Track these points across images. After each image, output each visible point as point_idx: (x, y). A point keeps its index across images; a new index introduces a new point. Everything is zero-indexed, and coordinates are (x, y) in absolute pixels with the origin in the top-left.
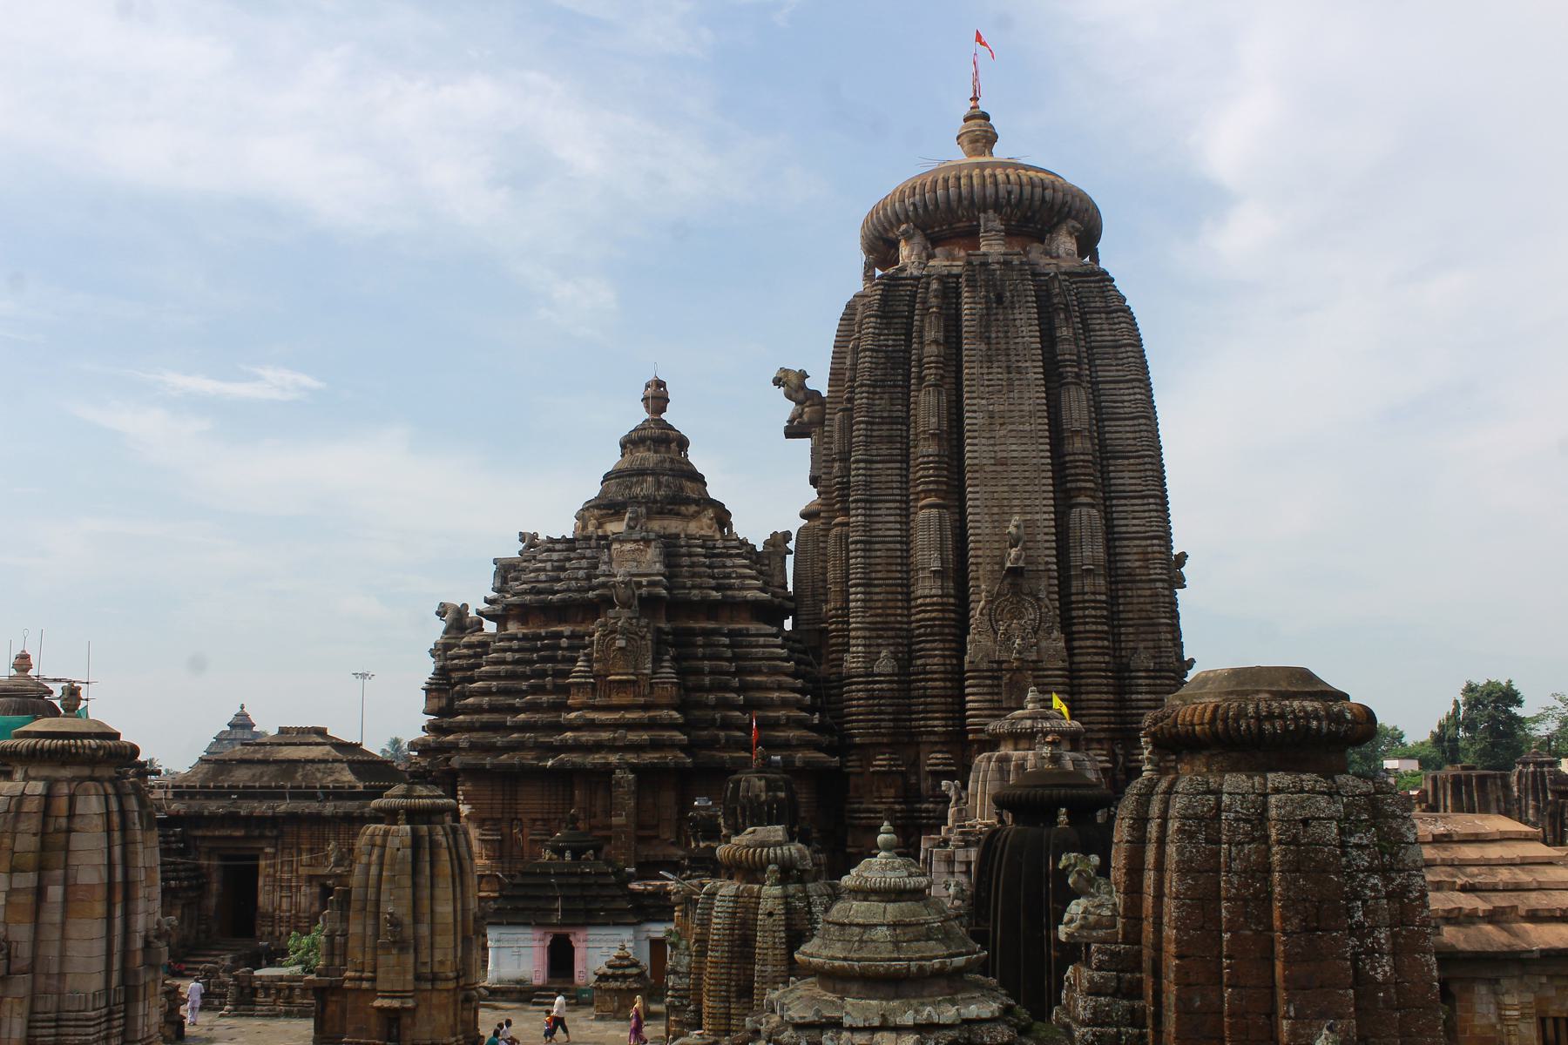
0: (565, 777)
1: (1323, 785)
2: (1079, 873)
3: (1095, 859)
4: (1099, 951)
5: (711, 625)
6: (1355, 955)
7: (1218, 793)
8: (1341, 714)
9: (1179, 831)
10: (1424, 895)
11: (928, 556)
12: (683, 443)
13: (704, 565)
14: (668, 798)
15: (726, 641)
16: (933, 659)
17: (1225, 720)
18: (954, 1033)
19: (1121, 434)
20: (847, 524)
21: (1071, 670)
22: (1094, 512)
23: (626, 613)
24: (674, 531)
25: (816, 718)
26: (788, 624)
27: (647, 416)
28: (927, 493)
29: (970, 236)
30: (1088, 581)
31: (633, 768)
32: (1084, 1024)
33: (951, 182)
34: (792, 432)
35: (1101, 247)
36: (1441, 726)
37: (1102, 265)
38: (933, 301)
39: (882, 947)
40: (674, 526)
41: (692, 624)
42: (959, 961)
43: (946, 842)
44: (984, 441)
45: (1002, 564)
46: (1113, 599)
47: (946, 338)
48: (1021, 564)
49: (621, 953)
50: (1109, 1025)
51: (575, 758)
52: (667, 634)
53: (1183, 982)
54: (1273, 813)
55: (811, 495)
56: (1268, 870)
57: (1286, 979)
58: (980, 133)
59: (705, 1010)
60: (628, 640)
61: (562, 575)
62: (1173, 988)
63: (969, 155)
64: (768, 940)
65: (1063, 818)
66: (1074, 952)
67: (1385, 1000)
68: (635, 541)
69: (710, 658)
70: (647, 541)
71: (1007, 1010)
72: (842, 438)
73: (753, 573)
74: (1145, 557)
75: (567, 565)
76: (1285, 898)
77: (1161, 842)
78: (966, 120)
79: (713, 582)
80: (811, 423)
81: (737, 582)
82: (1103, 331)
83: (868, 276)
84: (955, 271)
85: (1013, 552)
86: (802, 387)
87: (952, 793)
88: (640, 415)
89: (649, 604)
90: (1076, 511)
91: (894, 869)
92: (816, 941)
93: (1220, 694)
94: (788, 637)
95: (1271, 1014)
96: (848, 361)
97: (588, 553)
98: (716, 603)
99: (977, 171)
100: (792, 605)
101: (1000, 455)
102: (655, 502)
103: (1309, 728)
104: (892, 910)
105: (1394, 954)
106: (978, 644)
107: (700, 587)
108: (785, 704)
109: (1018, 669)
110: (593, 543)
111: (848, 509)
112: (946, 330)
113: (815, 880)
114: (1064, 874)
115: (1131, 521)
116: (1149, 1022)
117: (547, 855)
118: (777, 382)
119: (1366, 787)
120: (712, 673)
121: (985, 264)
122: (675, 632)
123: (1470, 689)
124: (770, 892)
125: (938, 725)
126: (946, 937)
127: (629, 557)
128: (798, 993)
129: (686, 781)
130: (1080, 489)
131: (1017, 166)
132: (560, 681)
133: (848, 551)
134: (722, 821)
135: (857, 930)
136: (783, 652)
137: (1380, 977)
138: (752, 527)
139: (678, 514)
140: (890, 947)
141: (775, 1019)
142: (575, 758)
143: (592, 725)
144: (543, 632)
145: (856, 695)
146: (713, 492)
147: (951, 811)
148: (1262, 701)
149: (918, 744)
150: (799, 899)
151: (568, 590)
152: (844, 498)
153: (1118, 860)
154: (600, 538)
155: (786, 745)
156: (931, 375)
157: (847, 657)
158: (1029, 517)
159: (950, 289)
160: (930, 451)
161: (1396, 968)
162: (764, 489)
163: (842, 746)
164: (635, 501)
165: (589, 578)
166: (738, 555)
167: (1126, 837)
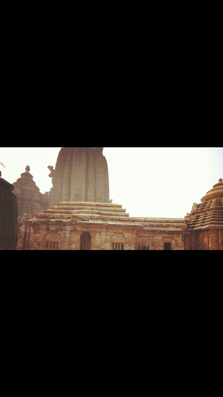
12: (32, 177)
34: (50, 176)
48: (78, 193)
70: (18, 188)
88: (25, 171)
101: (77, 176)
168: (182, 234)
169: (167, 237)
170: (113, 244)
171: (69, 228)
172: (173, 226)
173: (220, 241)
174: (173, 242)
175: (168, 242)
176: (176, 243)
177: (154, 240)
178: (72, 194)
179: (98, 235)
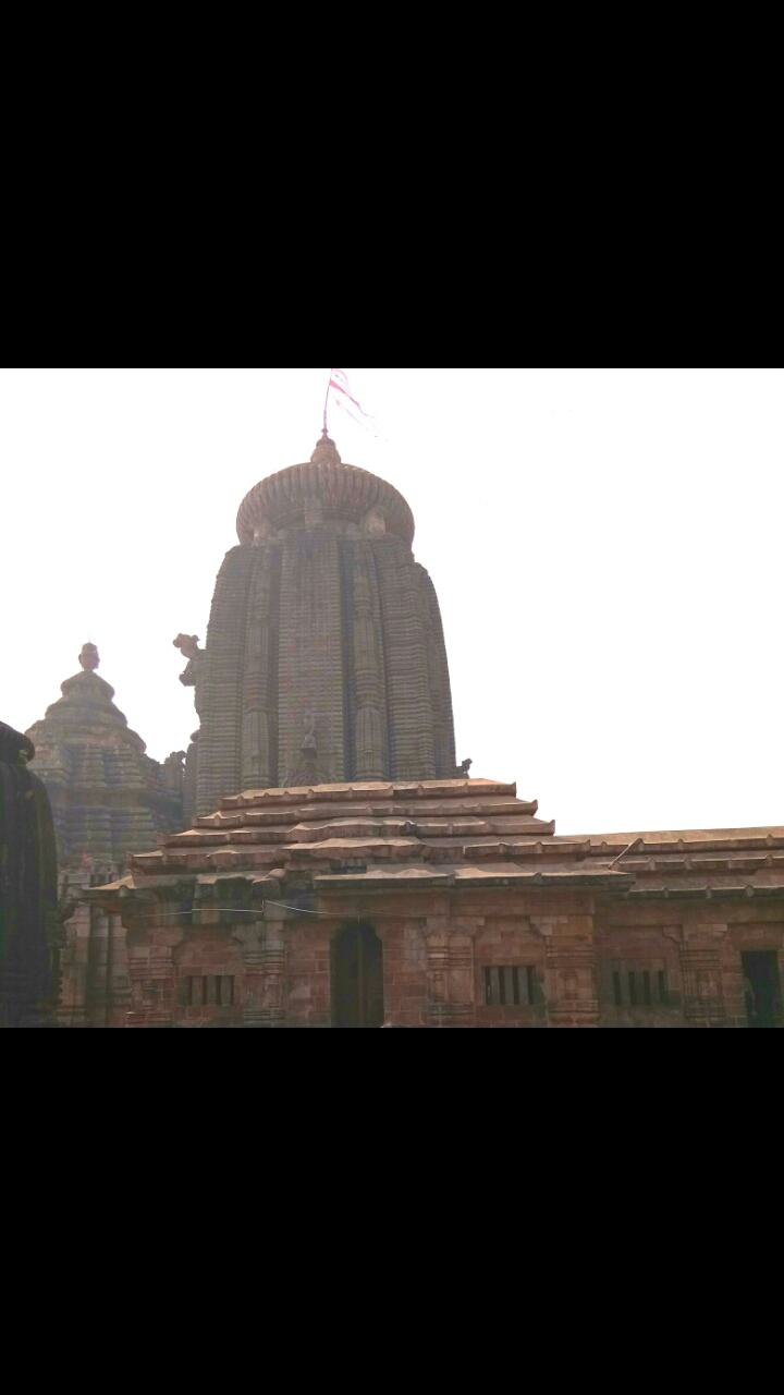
12: (107, 691)
22: (374, 711)
34: (186, 679)
44: (292, 659)
48: (311, 746)
70: (51, 746)
88: (78, 669)
130: (366, 695)
158: (323, 714)
170: (487, 970)
171: (277, 909)
177: (686, 939)
178: (284, 750)
179: (411, 934)
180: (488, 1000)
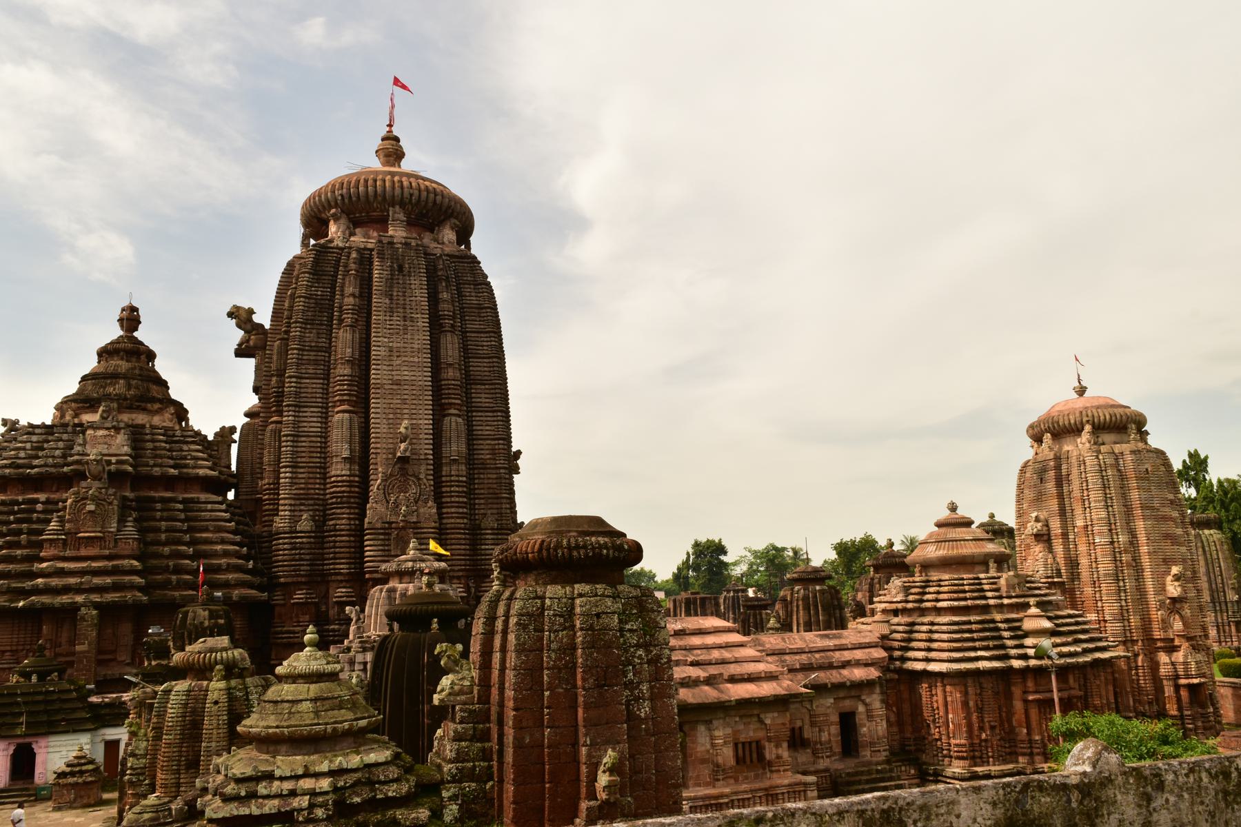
0: (34, 615)
1: (609, 591)
2: (449, 657)
3: (460, 647)
4: (461, 710)
5: (168, 495)
6: (628, 704)
7: (543, 598)
8: (621, 545)
9: (517, 624)
10: (669, 660)
11: (340, 447)
12: (151, 356)
13: (165, 449)
14: (126, 629)
15: (181, 506)
16: (342, 520)
17: (548, 549)
18: (358, 775)
19: (480, 367)
20: (281, 422)
21: (440, 529)
22: (460, 420)
23: (97, 484)
24: (140, 422)
25: (251, 564)
26: (231, 495)
27: (121, 333)
28: (342, 402)
29: (382, 223)
30: (454, 467)
31: (96, 606)
32: (450, 761)
33: (370, 182)
34: (240, 353)
35: (473, 239)
36: (679, 569)
37: (473, 252)
38: (353, 266)
39: (306, 716)
40: (141, 418)
41: (153, 494)
42: (363, 723)
43: (349, 649)
45: (394, 454)
46: (471, 479)
47: (361, 293)
48: (408, 454)
49: (80, 754)
50: (468, 761)
51: (46, 599)
52: (132, 501)
53: (518, 727)
54: (578, 610)
55: (254, 400)
56: (574, 648)
57: (585, 720)
58: (392, 151)
59: (159, 782)
60: (97, 505)
61: (40, 454)
62: (511, 731)
63: (384, 165)
64: (213, 723)
65: (435, 626)
66: (442, 713)
67: (646, 730)
68: (107, 429)
69: (167, 520)
70: (117, 429)
71: (397, 756)
72: (279, 359)
73: (205, 456)
74: (493, 452)
75: (46, 445)
76: (584, 666)
77: (505, 632)
78: (383, 139)
79: (171, 462)
80: (256, 347)
81: (191, 462)
82: (472, 298)
83: (305, 244)
84: (370, 246)
85: (403, 446)
86: (251, 320)
87: (353, 616)
88: (116, 332)
89: (116, 478)
90: (447, 419)
91: (316, 659)
92: (254, 716)
93: (545, 533)
94: (230, 505)
95: (575, 744)
96: (286, 304)
97: (65, 436)
98: (174, 477)
99: (388, 177)
100: (235, 481)
102: (126, 399)
103: (601, 554)
104: (314, 689)
105: (651, 699)
106: (375, 511)
107: (161, 466)
108: (226, 554)
109: (404, 528)
110: (70, 429)
111: (282, 411)
112: (361, 288)
113: (252, 676)
114: (438, 658)
115: (485, 428)
116: (495, 757)
117: (14, 679)
118: (230, 315)
119: (637, 592)
120: (166, 531)
121: (391, 243)
122: (138, 499)
123: (697, 545)
124: (216, 687)
125: (344, 568)
126: (354, 706)
127: (101, 440)
128: (239, 757)
129: (140, 615)
131: (418, 177)
132: (33, 538)
133: (280, 441)
134: (171, 644)
135: (287, 705)
136: (227, 515)
137: (643, 715)
138: (206, 422)
139: (144, 410)
140: (312, 715)
141: (220, 778)
142: (46, 599)
143: (61, 573)
144: (20, 498)
145: (282, 548)
146: (174, 394)
147: (352, 628)
148: (572, 538)
149: (328, 582)
150: (239, 690)
151: (46, 465)
152: (279, 403)
153: (475, 646)
154: (76, 425)
155: (226, 585)
156: (348, 318)
157: (277, 519)
159: (365, 259)
160: (346, 372)
161: (653, 709)
162: (216, 395)
163: (270, 584)
164: (108, 397)
165: (64, 456)
166: (193, 442)
167: (481, 631)
168: (881, 686)
169: (844, 698)
170: (736, 745)
172: (858, 663)
173: (971, 704)
174: (861, 708)
175: (848, 710)
176: (868, 711)
180: (738, 762)
